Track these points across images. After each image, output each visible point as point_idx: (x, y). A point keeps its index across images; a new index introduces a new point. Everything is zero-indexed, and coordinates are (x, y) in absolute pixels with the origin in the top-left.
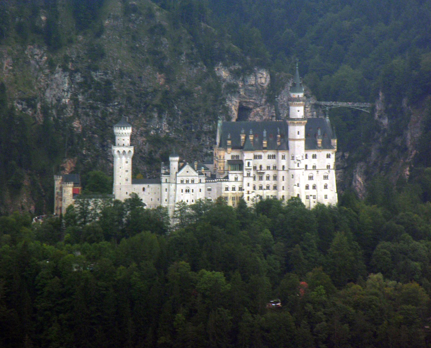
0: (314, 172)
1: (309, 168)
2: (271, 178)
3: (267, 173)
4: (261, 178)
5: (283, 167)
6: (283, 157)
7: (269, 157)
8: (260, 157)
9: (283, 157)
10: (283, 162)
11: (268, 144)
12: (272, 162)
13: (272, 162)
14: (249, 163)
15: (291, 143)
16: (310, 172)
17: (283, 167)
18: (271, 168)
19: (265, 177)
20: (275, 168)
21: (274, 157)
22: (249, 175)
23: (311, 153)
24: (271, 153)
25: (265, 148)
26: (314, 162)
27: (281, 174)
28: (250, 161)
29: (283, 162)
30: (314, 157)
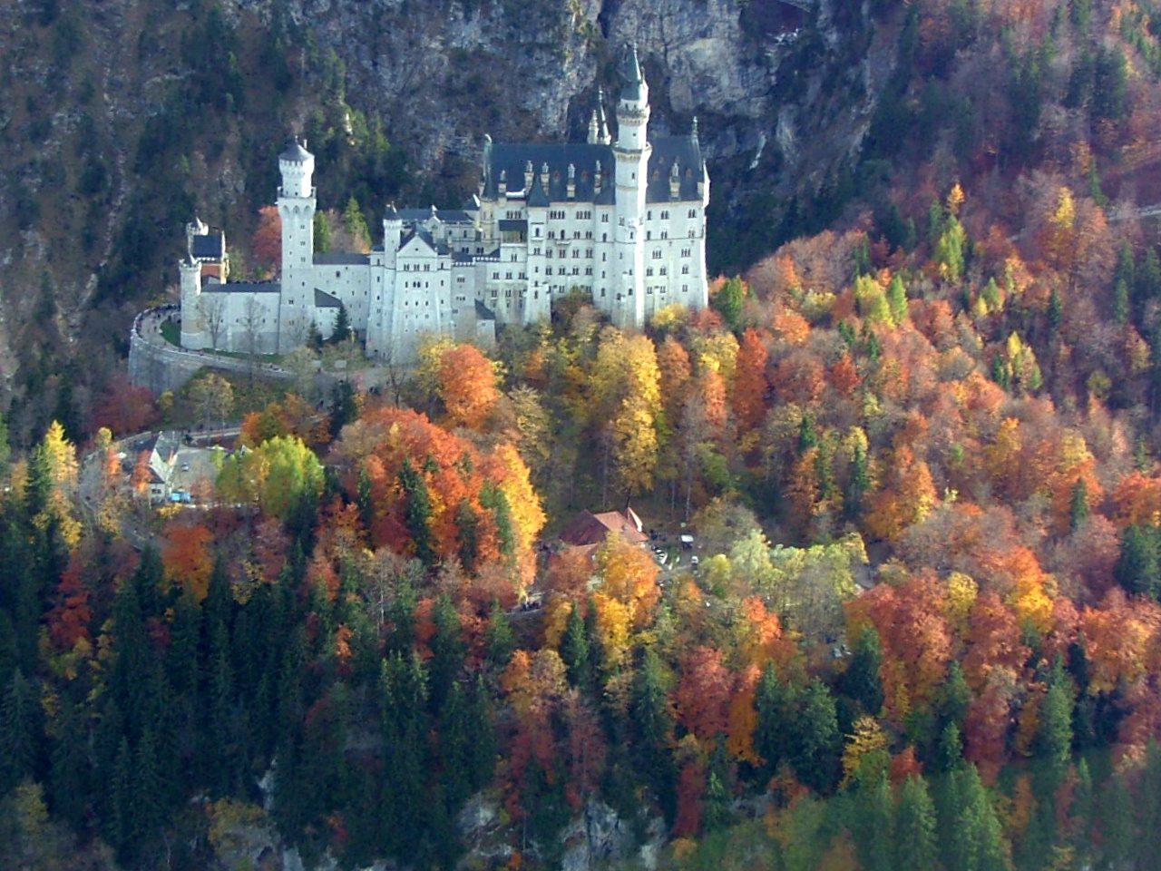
0: (665, 243)
1: (652, 237)
2: (582, 254)
3: (575, 244)
4: (562, 254)
5: (605, 236)
6: (605, 218)
7: (579, 216)
8: (562, 215)
9: (605, 218)
10: (604, 228)
11: (576, 191)
12: (583, 225)
13: (583, 225)
14: (537, 231)
15: (618, 192)
16: (656, 243)
17: (605, 236)
18: (583, 235)
19: (569, 253)
20: (589, 235)
21: (588, 215)
22: (537, 252)
23: (658, 209)
24: (583, 207)
25: (571, 200)
26: (665, 225)
27: (600, 248)
28: (541, 227)
29: (604, 228)
30: (665, 216)
